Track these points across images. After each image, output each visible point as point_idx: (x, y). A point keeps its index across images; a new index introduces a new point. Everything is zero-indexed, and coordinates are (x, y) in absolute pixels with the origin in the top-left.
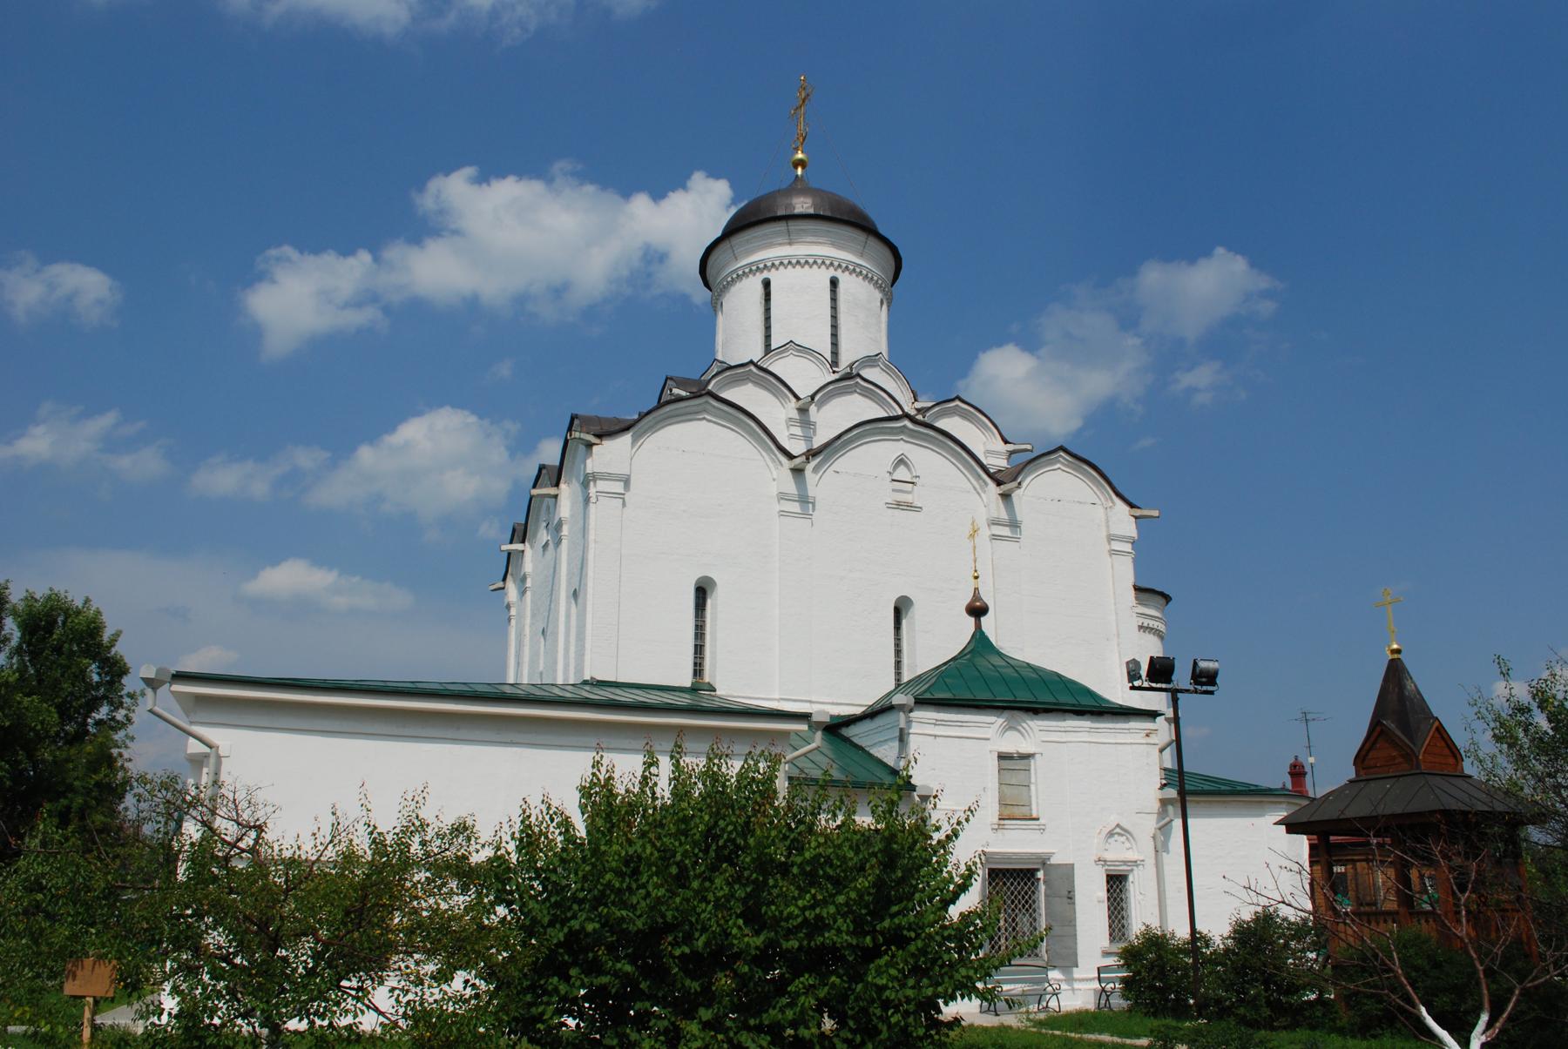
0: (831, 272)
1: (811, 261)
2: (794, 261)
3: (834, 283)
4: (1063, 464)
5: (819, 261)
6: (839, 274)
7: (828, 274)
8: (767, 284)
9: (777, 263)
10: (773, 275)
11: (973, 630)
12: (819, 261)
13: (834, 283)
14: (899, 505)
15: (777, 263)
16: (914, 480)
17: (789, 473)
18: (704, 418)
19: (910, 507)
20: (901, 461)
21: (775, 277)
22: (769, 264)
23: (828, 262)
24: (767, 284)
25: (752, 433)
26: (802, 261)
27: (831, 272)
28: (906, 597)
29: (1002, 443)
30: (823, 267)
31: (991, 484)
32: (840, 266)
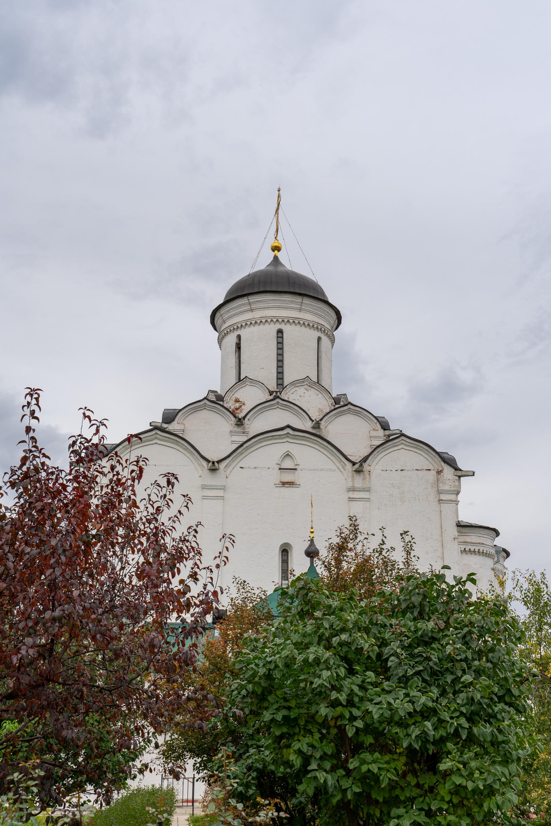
0: (278, 326)
1: (264, 321)
2: (253, 322)
3: (280, 331)
4: (405, 445)
5: (269, 320)
6: (282, 326)
7: (273, 329)
8: (239, 337)
9: (244, 324)
10: (242, 332)
11: (309, 565)
12: (269, 320)
13: (280, 331)
14: (284, 484)
15: (244, 324)
16: (296, 467)
17: (208, 471)
18: (156, 443)
19: (291, 484)
20: (288, 455)
21: (245, 333)
22: (239, 325)
23: (275, 320)
24: (239, 337)
25: (186, 449)
26: (258, 321)
27: (278, 326)
28: (287, 543)
29: (382, 431)
30: (272, 323)
31: (349, 465)
32: (283, 321)
